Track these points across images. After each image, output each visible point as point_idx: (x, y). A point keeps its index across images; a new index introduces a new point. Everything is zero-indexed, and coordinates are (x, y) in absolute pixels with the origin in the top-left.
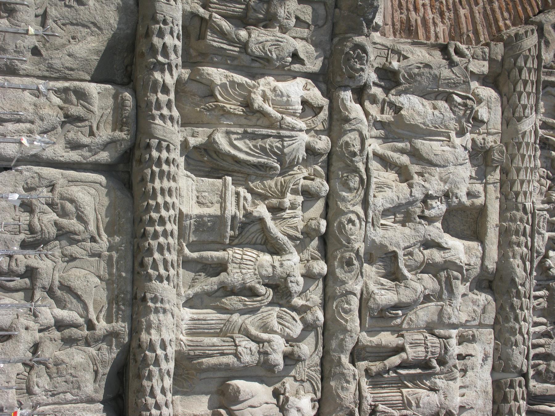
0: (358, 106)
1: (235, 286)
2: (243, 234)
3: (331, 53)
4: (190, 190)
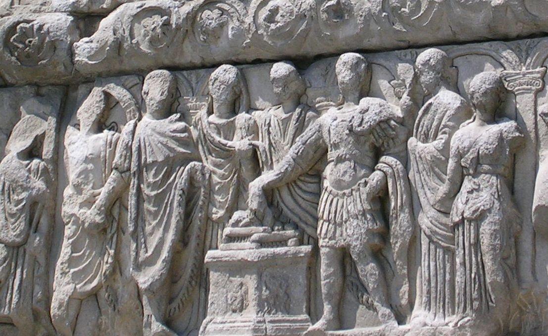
0: (104, 22)
1: (368, 231)
2: (296, 220)
3: (29, 84)
4: (221, 326)
